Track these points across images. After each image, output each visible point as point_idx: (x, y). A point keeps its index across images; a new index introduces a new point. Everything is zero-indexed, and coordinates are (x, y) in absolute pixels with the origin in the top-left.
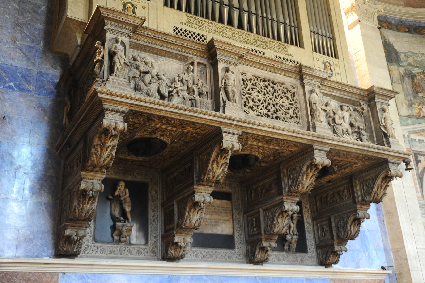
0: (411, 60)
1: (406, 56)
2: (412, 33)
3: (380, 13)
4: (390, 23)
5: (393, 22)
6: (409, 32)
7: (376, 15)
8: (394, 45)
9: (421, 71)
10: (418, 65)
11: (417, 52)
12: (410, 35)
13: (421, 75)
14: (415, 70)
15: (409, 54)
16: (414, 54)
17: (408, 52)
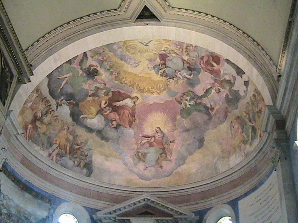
0: (5, 202)
1: (4, 197)
2: (14, 183)
3: (6, 161)
4: (7, 170)
5: (9, 169)
6: (13, 181)
7: (4, 160)
8: (1, 186)
9: (6, 212)
10: (7, 208)
11: (11, 198)
12: (13, 184)
13: (5, 216)
14: (3, 210)
15: (6, 196)
16: (9, 198)
17: (6, 195)
